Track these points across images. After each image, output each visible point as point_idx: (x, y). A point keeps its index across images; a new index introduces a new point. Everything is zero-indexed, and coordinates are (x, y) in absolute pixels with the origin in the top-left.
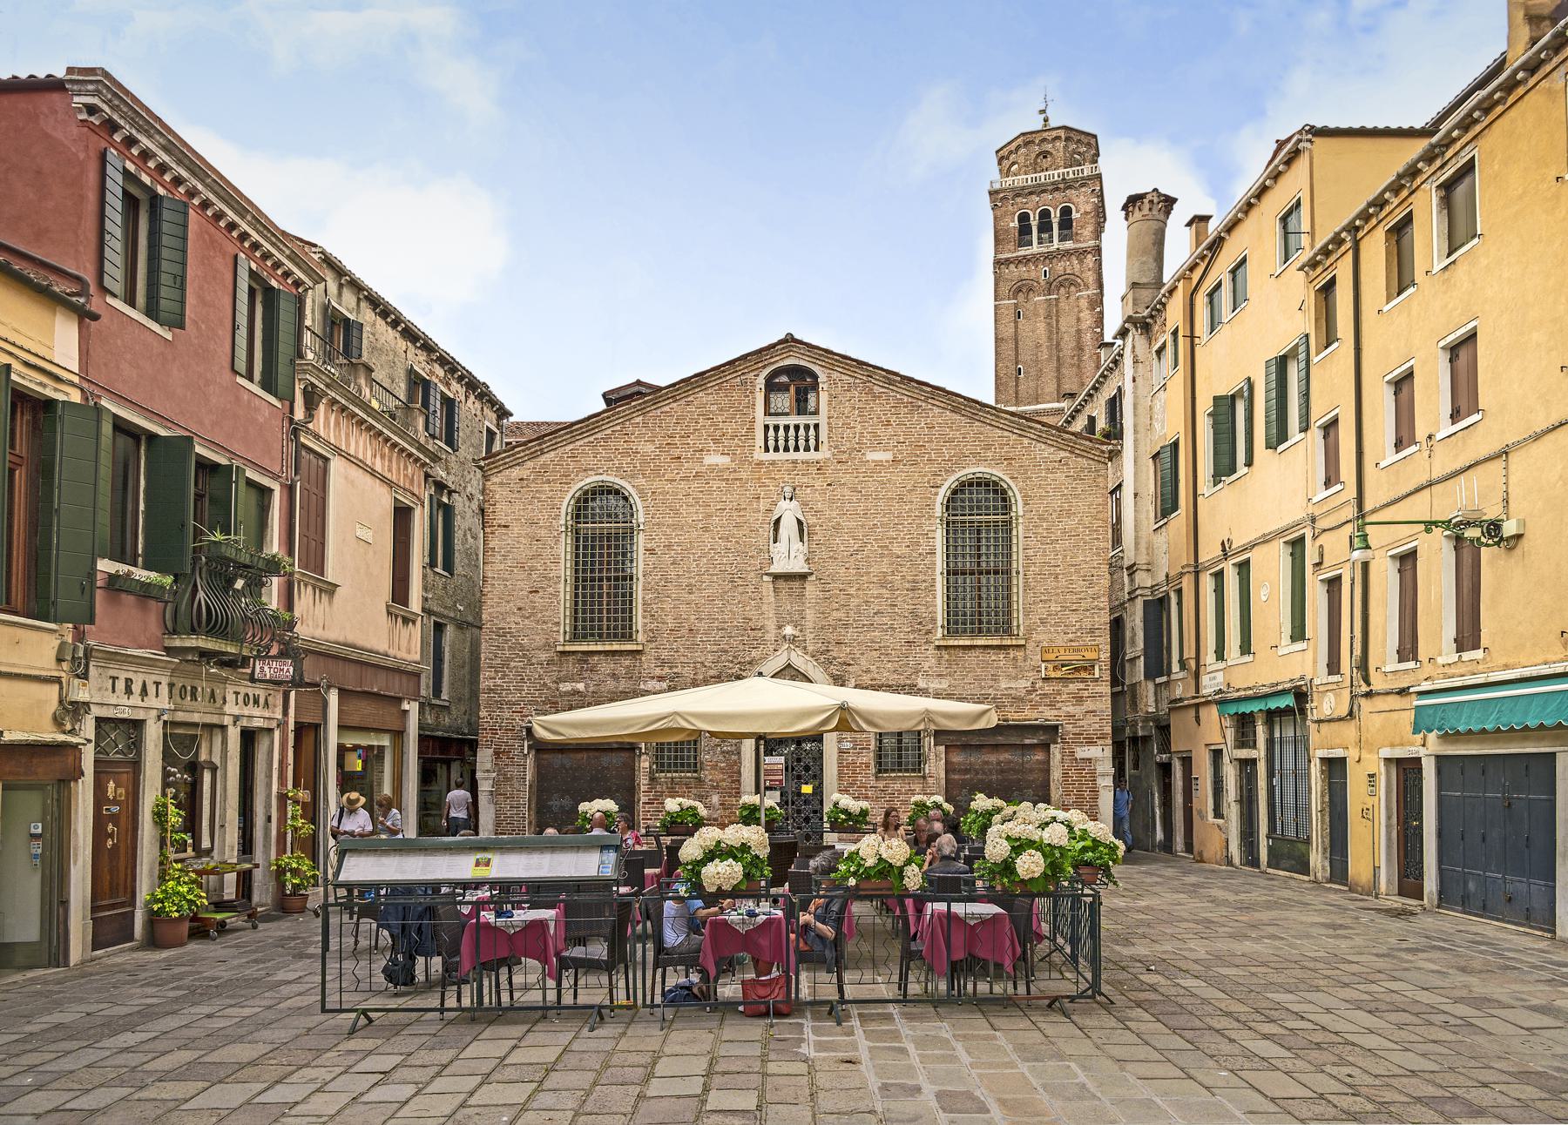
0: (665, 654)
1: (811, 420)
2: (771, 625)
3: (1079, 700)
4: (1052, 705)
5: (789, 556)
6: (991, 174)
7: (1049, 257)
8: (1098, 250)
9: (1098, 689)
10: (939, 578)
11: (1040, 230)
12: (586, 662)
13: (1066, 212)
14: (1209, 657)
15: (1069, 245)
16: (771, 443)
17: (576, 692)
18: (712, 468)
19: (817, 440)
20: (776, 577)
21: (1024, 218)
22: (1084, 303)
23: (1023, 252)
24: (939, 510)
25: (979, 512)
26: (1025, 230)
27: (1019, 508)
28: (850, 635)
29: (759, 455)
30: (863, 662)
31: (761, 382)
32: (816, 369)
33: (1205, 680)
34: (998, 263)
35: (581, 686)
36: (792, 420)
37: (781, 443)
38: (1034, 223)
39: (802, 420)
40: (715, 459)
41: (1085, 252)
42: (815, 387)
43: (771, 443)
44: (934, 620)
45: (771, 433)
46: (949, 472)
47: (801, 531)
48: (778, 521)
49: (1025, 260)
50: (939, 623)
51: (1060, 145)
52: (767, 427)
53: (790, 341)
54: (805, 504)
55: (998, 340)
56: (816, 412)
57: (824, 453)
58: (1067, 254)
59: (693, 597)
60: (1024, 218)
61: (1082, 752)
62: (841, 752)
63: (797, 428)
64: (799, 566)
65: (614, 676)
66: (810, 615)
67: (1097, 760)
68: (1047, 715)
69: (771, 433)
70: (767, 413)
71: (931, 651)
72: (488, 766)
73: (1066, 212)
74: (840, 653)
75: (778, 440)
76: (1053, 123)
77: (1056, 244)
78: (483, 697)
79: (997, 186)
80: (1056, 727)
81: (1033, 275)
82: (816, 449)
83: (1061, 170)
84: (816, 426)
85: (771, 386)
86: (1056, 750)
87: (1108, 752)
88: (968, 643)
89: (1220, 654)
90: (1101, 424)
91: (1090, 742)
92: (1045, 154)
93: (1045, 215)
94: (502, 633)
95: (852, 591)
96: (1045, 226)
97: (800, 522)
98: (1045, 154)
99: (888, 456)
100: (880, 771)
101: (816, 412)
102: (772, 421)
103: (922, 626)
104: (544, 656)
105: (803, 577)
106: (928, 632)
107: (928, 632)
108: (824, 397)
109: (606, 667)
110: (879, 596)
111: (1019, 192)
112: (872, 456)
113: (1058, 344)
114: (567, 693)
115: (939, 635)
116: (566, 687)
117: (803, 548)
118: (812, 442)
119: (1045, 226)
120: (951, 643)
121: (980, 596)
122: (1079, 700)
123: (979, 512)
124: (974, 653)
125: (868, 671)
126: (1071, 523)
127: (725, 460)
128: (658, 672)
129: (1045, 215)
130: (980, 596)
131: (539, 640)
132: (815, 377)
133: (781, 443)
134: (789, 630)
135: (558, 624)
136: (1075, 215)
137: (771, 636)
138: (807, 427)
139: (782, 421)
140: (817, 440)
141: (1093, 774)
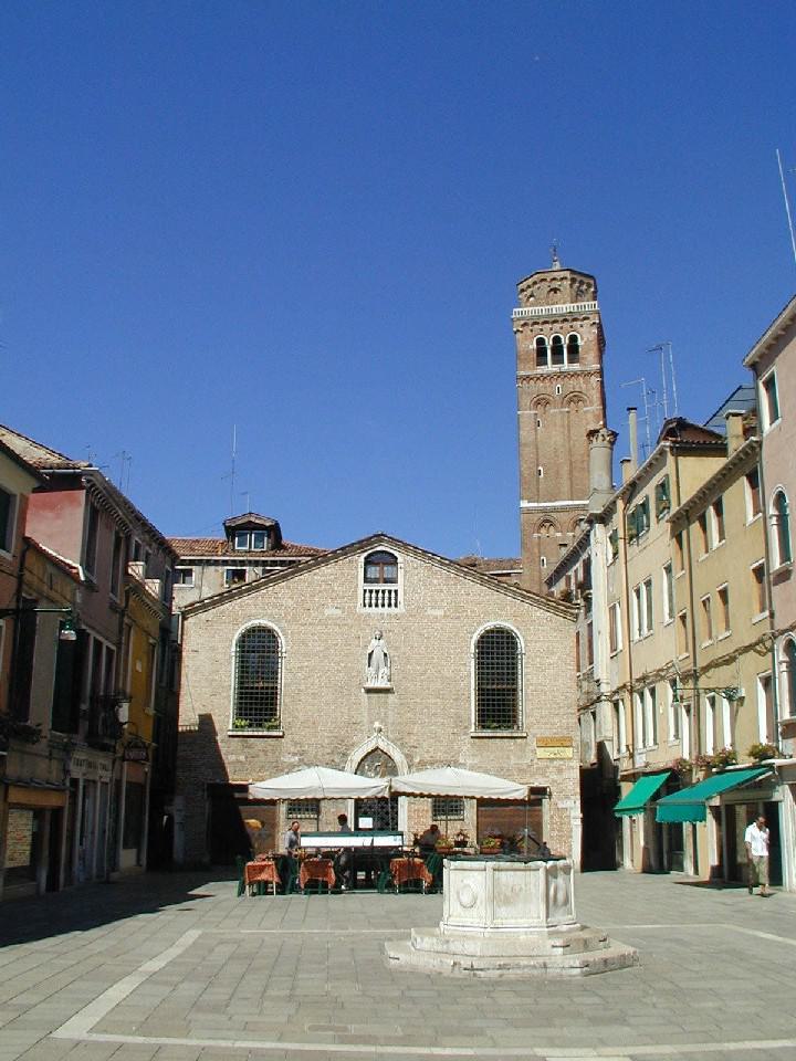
0: (297, 738)
3: (560, 771)
4: (544, 775)
7: (561, 375)
9: (571, 764)
10: (473, 692)
11: (553, 353)
12: (246, 742)
13: (573, 339)
15: (576, 367)
16: (367, 602)
18: (328, 618)
19: (396, 600)
20: (369, 691)
21: (541, 342)
23: (542, 370)
25: (497, 652)
26: (541, 352)
31: (362, 559)
32: (396, 554)
33: (637, 757)
35: (242, 758)
37: (373, 602)
38: (549, 344)
40: (327, 612)
41: (590, 374)
43: (367, 602)
44: (470, 719)
45: (368, 594)
46: (479, 624)
47: (386, 660)
48: (370, 655)
49: (542, 378)
50: (473, 721)
51: (567, 283)
52: (365, 591)
53: (379, 538)
54: (388, 642)
57: (401, 609)
58: (575, 374)
59: (316, 701)
60: (541, 342)
63: (383, 592)
64: (382, 684)
67: (571, 808)
69: (368, 594)
70: (366, 580)
71: (468, 739)
72: (181, 807)
73: (573, 339)
75: (373, 600)
77: (566, 366)
78: (179, 763)
80: (545, 789)
81: (549, 391)
82: (396, 606)
83: (568, 305)
84: (396, 592)
85: (368, 562)
86: (545, 802)
87: (578, 803)
88: (491, 735)
91: (567, 797)
92: (555, 290)
93: (557, 340)
95: (418, 700)
96: (557, 350)
97: (385, 655)
98: (555, 290)
100: (435, 815)
103: (459, 721)
105: (387, 691)
106: (466, 727)
107: (466, 727)
108: (401, 573)
110: (436, 704)
113: (570, 450)
114: (233, 763)
115: (473, 730)
117: (386, 670)
118: (393, 602)
119: (557, 350)
120: (480, 735)
121: (498, 706)
123: (497, 652)
125: (428, 752)
126: (555, 658)
127: (339, 612)
128: (292, 749)
129: (557, 340)
130: (498, 706)
132: (396, 558)
133: (373, 602)
134: (377, 725)
135: (228, 716)
136: (580, 342)
137: (365, 728)
138: (390, 592)
139: (374, 587)
140: (396, 600)
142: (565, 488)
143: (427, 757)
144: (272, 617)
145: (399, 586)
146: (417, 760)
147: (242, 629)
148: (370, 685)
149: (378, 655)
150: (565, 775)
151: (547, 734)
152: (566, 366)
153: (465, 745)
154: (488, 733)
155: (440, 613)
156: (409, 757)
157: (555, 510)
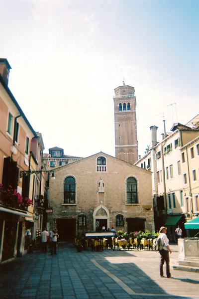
0: (80, 206)
1: (105, 166)
2: (98, 201)
3: (149, 215)
4: (144, 215)
5: (102, 189)
6: (113, 95)
8: (135, 112)
13: (129, 104)
14: (168, 208)
15: (129, 111)
17: (65, 213)
21: (120, 104)
22: (133, 124)
23: (120, 112)
24: (126, 182)
27: (138, 182)
28: (111, 203)
29: (96, 172)
30: (114, 208)
34: (115, 114)
35: (65, 211)
36: (101, 166)
39: (103, 166)
40: (89, 172)
42: (105, 160)
49: (121, 114)
55: (115, 131)
56: (105, 165)
58: (129, 113)
60: (120, 104)
61: (150, 223)
62: (110, 223)
65: (72, 210)
66: (105, 199)
68: (144, 217)
73: (129, 104)
74: (110, 206)
75: (99, 169)
76: (126, 85)
79: (115, 97)
85: (98, 160)
86: (145, 223)
89: (170, 207)
90: (147, 164)
91: (151, 221)
93: (125, 104)
94: (52, 202)
99: (117, 173)
101: (105, 165)
102: (98, 166)
103: (123, 202)
104: (59, 206)
109: (70, 208)
111: (119, 99)
112: (114, 172)
116: (63, 211)
122: (149, 215)
124: (131, 207)
129: (125, 104)
131: (58, 203)
139: (100, 166)
141: (152, 227)
142: (127, 142)
143: (114, 211)
144: (73, 174)
145: (106, 166)
146: (112, 211)
147: (65, 177)
148: (100, 191)
149: (101, 184)
150: (150, 215)
151: (145, 204)
152: (127, 111)
153: (124, 207)
154: (130, 204)
155: (117, 173)
156: (110, 211)
157: (125, 147)
